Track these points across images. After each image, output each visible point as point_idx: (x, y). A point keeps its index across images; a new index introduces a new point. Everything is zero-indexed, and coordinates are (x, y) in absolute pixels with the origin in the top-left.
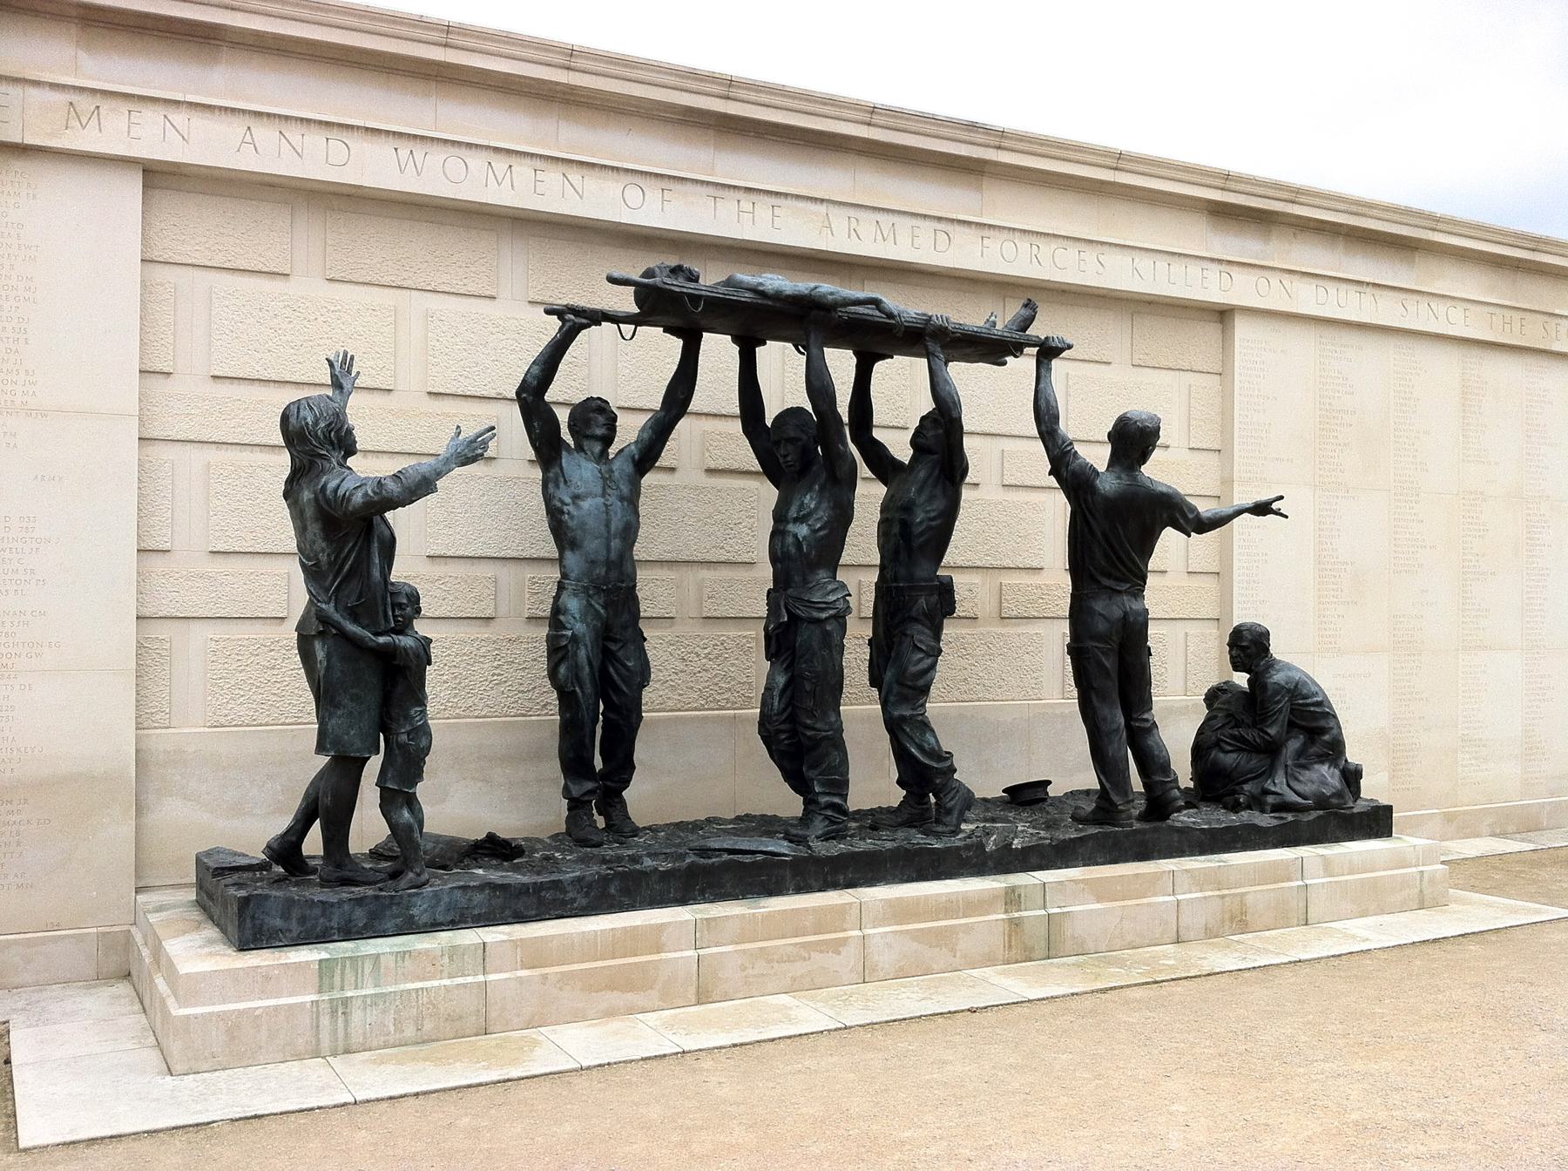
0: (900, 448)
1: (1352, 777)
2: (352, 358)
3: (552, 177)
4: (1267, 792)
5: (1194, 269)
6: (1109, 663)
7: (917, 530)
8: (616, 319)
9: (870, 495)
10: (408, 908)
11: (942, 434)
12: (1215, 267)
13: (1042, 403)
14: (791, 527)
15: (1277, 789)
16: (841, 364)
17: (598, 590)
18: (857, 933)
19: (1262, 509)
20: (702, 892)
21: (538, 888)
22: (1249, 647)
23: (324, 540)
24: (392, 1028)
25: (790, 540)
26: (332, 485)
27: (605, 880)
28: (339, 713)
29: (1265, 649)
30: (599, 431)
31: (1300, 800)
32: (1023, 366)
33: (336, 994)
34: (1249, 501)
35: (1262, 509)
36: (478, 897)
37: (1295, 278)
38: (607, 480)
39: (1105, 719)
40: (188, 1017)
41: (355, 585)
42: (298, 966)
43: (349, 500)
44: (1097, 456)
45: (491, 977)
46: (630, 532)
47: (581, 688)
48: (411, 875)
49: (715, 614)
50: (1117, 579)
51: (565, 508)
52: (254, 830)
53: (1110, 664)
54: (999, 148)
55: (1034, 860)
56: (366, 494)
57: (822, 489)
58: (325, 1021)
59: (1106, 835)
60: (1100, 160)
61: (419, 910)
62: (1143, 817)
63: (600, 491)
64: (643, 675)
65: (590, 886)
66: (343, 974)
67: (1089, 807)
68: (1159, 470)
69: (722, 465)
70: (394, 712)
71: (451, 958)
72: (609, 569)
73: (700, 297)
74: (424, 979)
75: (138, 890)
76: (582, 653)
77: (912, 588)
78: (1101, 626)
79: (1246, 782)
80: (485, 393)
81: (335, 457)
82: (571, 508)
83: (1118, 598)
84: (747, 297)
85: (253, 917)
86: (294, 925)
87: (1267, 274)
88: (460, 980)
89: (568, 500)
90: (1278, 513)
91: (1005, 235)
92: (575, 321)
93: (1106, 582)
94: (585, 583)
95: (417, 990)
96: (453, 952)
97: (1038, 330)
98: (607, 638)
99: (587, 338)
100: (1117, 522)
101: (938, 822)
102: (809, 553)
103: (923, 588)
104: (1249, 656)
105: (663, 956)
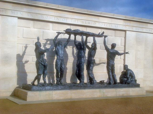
0: (90, 45)
1: (136, 81)
9: (87, 51)
11: (94, 44)
16: (85, 37)
22: (125, 67)
29: (127, 67)
44: (110, 47)
53: (111, 68)
62: (114, 84)
68: (116, 49)
90: (128, 53)
100: (112, 54)
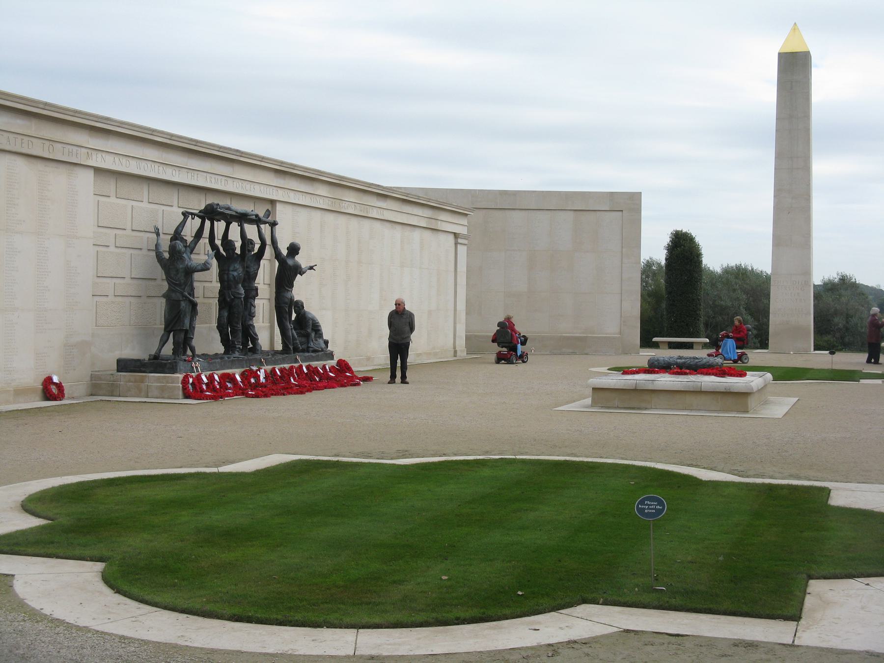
1: (326, 343)
19: (311, 268)
35: (311, 268)
68: (301, 259)
78: (287, 300)
100: (287, 273)
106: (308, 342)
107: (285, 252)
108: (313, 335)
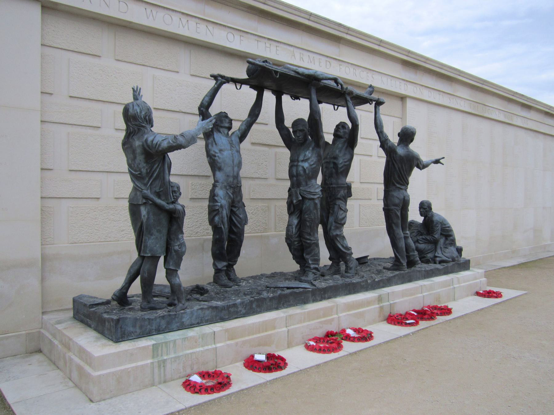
2: (140, 89)
3: (202, 27)
4: (436, 257)
5: (398, 82)
6: (399, 214)
7: (340, 166)
8: (235, 81)
10: (181, 319)
12: (403, 82)
13: (378, 121)
14: (300, 164)
15: (439, 256)
17: (230, 187)
18: (336, 316)
19: (437, 162)
20: (283, 304)
21: (229, 307)
22: (425, 208)
23: (145, 163)
24: (182, 370)
25: (300, 168)
26: (150, 139)
27: (251, 302)
28: (153, 237)
29: (431, 209)
30: (227, 125)
31: (447, 259)
32: (370, 107)
33: (160, 359)
34: (434, 159)
35: (437, 162)
36: (207, 312)
37: (423, 88)
38: (231, 144)
39: (398, 234)
40: (100, 376)
41: (158, 183)
42: (144, 348)
43: (160, 145)
45: (218, 345)
46: (240, 165)
47: (224, 226)
48: (181, 305)
49: (255, 198)
50: (401, 185)
51: (217, 155)
52: (106, 287)
54: (347, 34)
55: (381, 284)
56: (169, 142)
57: (313, 149)
58: (156, 370)
59: (400, 274)
60: (375, 42)
61: (186, 320)
63: (230, 149)
64: (245, 221)
65: (246, 305)
66: (162, 349)
67: (389, 265)
68: (416, 147)
69: (257, 142)
70: (172, 237)
71: (202, 339)
72: (234, 179)
73: (278, 72)
74: (192, 348)
75: (43, 313)
76: (224, 212)
77: (339, 187)
78: (397, 201)
79: (428, 253)
80: (175, 110)
81: (148, 126)
82: (219, 155)
83: (401, 191)
84: (292, 74)
85: (121, 328)
86: (138, 331)
87: (416, 85)
88: (206, 348)
89: (217, 151)
91: (346, 64)
92: (221, 80)
93: (398, 186)
94: (225, 184)
95: (191, 353)
96: (203, 336)
97: (375, 96)
98: (233, 206)
99: (228, 88)
100: (399, 166)
101: (346, 272)
102: (309, 174)
103: (342, 187)
104: (426, 211)
105: (276, 331)
106: (435, 250)
107: (394, 139)
108: (442, 241)
